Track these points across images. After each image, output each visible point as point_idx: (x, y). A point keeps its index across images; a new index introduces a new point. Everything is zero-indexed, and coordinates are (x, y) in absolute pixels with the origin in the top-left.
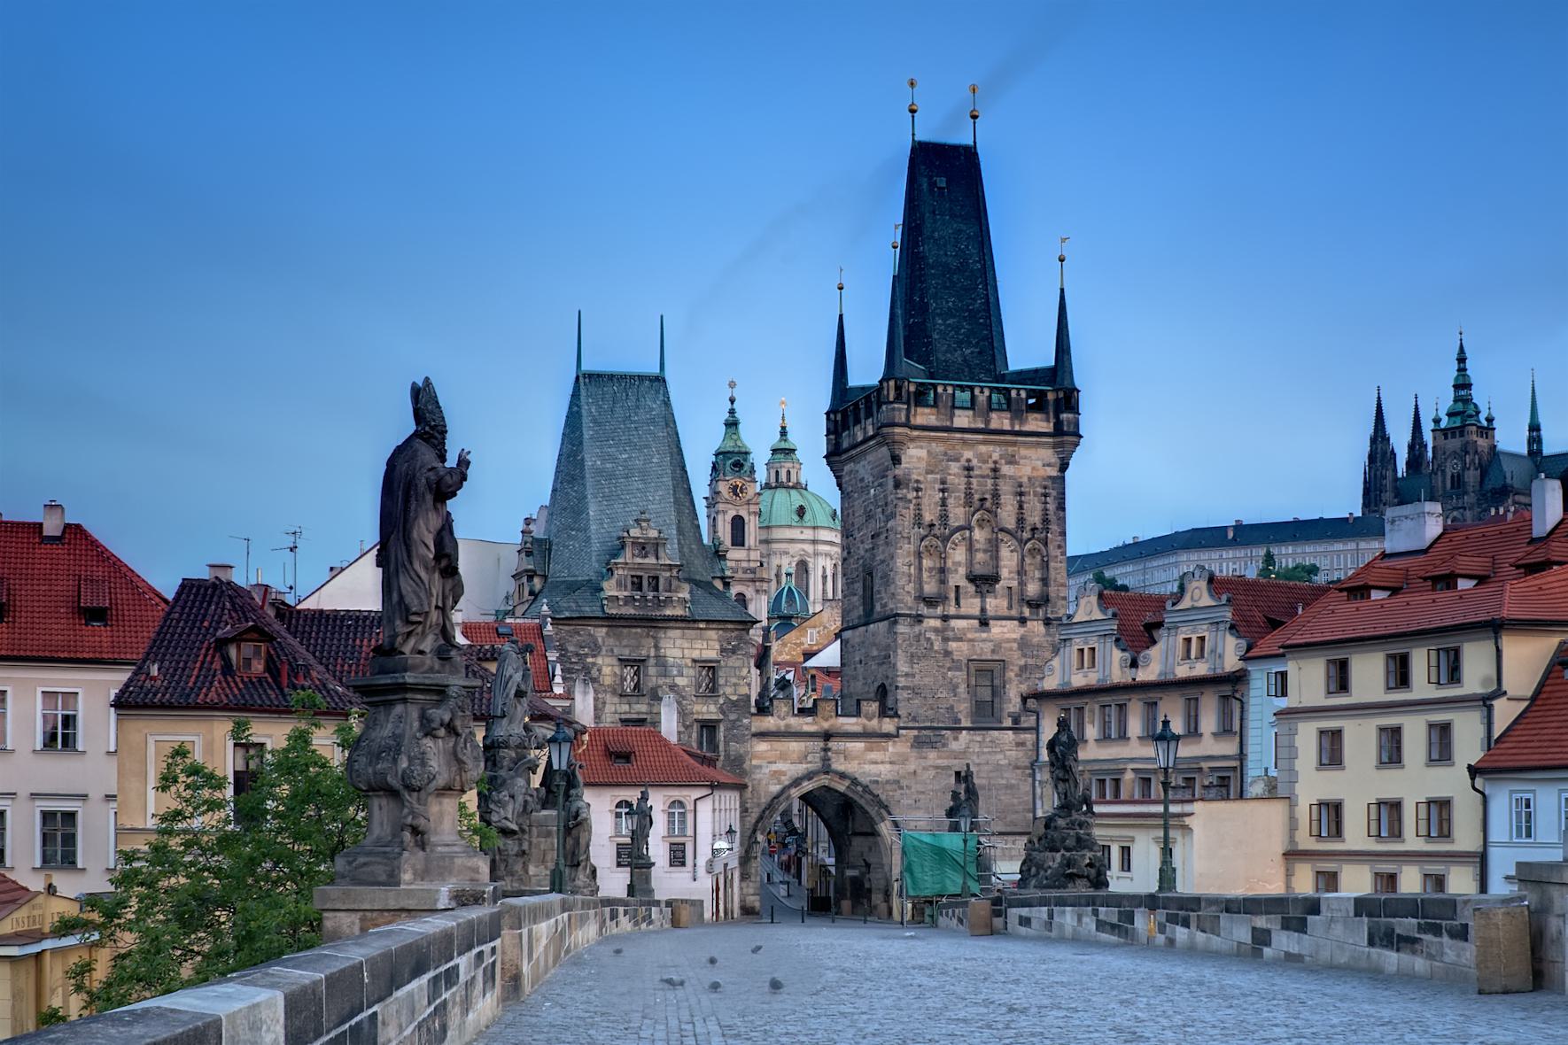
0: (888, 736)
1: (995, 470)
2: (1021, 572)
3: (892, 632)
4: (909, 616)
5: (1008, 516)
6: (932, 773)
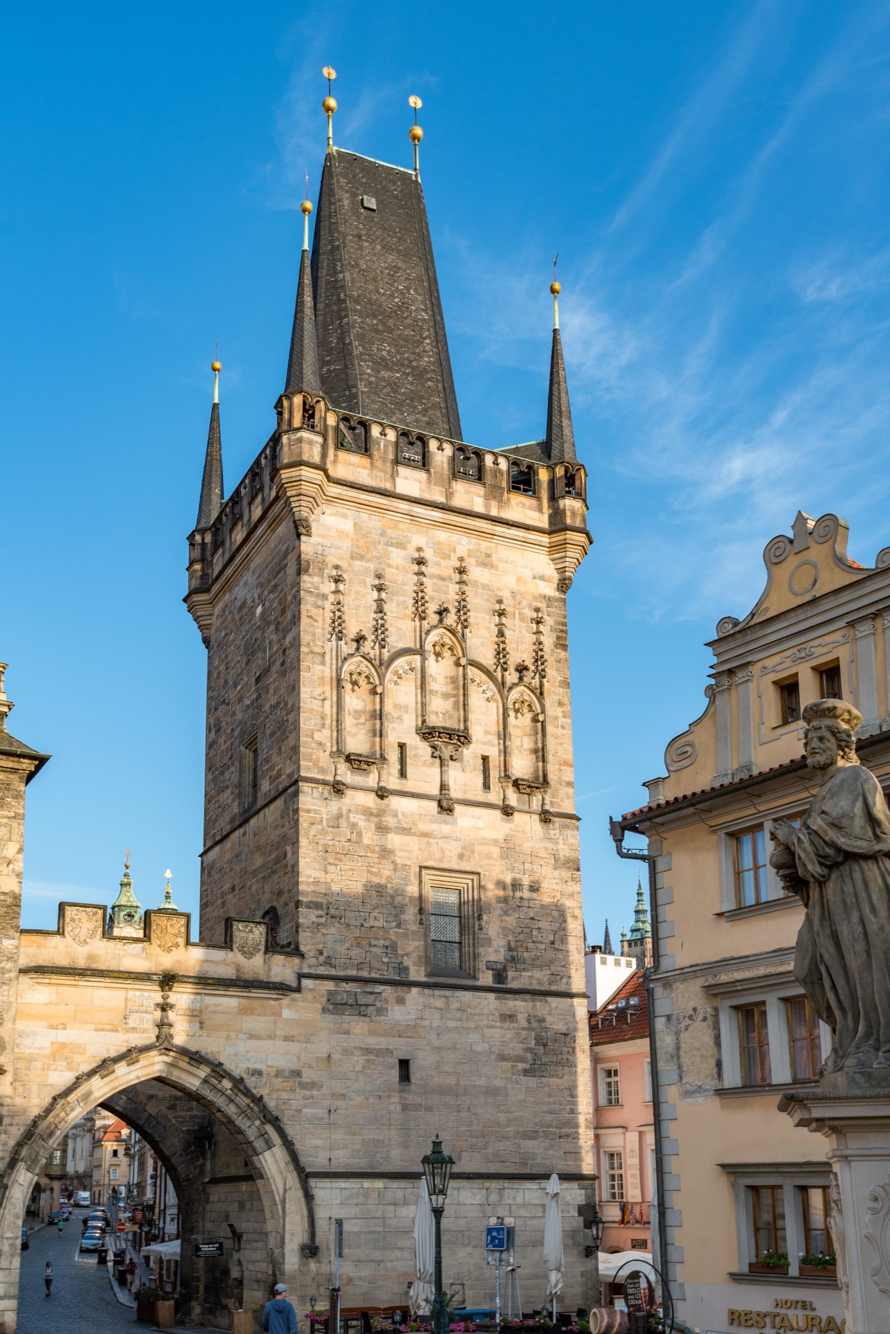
0: (282, 988)
1: (462, 571)
2: (504, 735)
3: (292, 814)
4: (325, 783)
5: (481, 644)
6: (359, 1060)
